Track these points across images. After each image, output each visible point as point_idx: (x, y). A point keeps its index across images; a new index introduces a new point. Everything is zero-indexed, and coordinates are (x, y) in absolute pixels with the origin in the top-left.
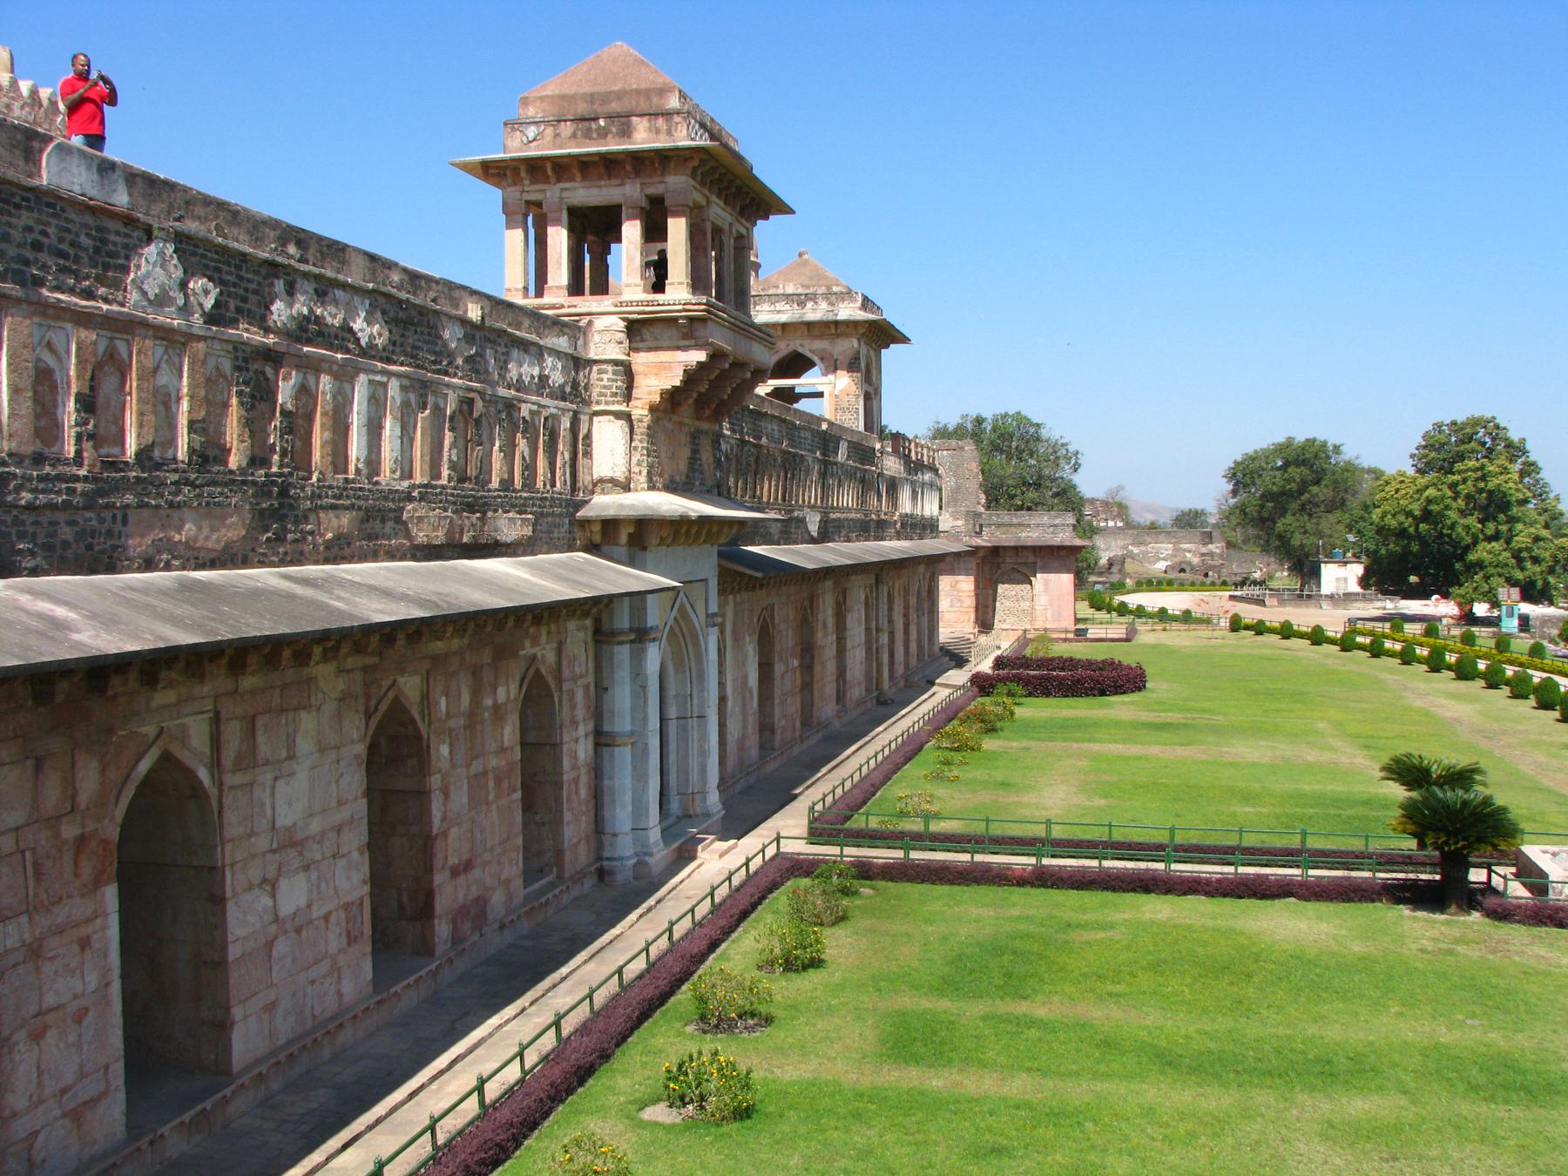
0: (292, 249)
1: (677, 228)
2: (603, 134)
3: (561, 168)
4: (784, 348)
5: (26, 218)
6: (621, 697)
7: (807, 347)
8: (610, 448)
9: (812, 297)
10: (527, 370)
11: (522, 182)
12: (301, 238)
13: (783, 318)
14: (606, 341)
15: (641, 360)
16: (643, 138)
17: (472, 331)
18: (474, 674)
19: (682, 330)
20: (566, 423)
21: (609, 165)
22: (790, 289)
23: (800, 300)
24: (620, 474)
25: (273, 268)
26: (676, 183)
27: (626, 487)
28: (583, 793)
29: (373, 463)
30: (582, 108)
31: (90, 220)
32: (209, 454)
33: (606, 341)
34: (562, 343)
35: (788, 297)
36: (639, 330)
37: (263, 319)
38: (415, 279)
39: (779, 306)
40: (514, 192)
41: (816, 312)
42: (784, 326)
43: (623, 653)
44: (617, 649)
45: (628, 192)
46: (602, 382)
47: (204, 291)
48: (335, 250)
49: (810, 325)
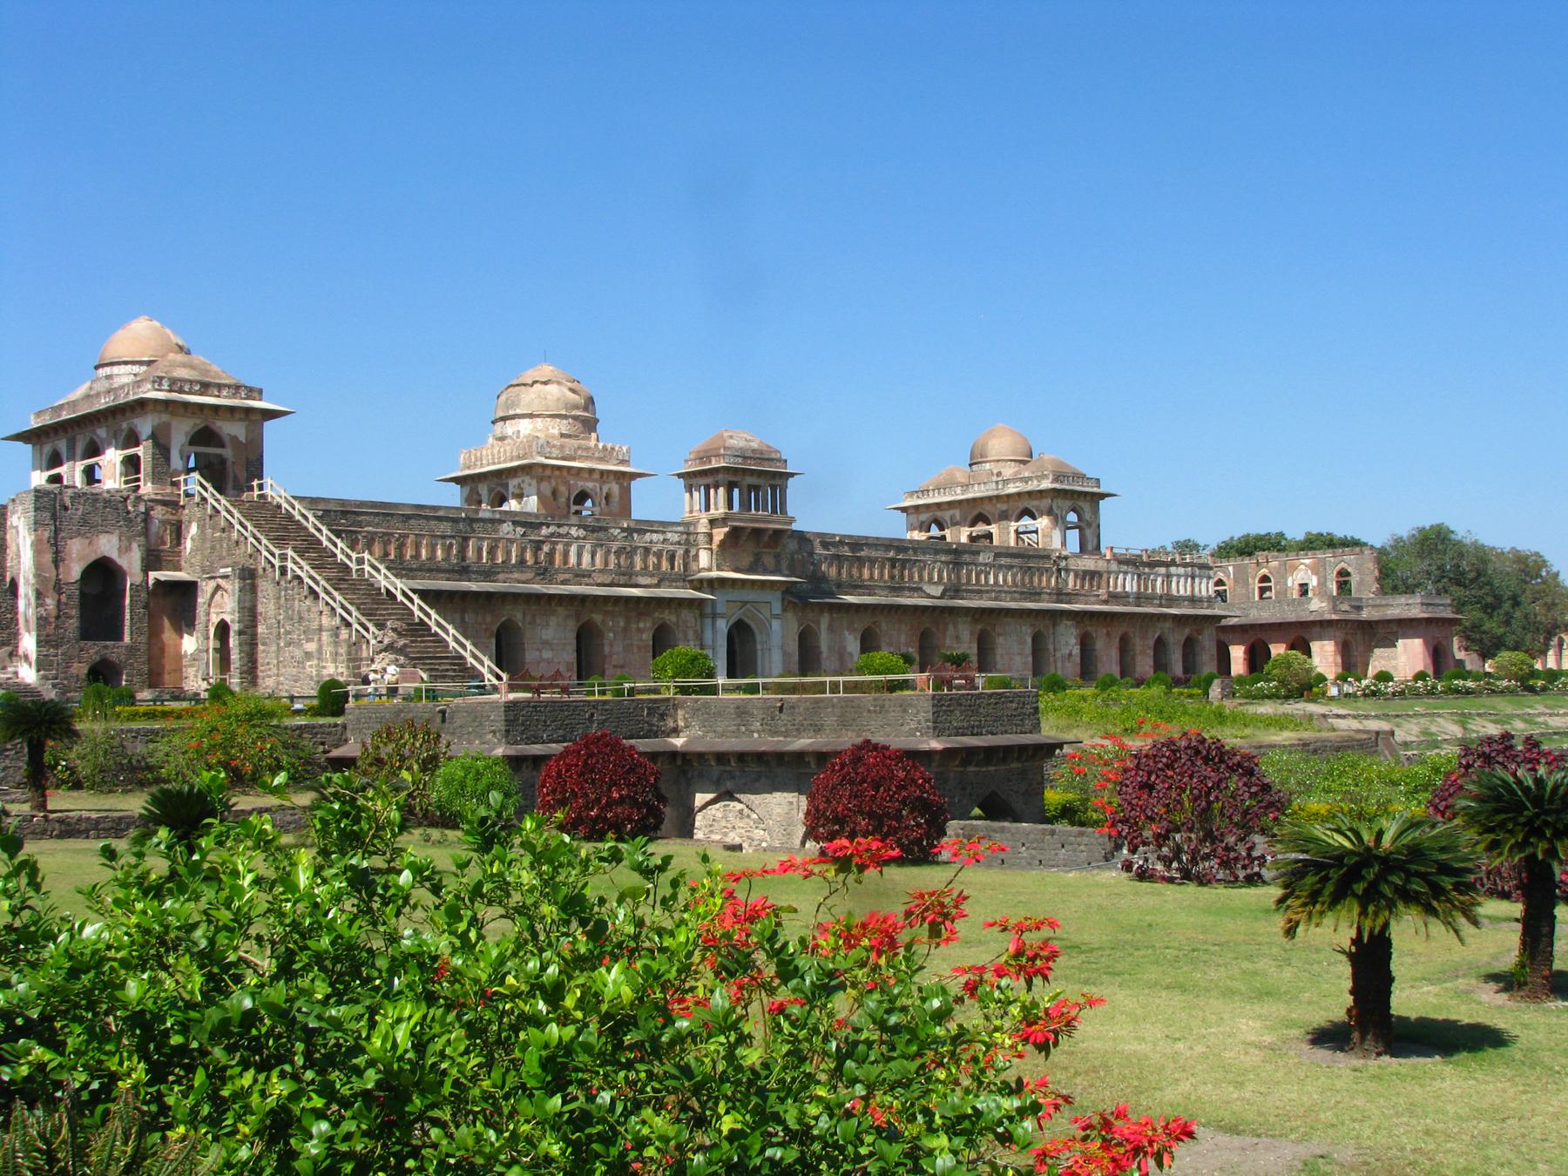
1: (736, 491)
4: (1022, 505)
6: (708, 635)
7: (1031, 504)
8: (704, 559)
9: (1030, 478)
11: (690, 479)
14: (703, 528)
15: (715, 531)
16: (715, 464)
19: (723, 521)
20: (680, 552)
26: (720, 477)
27: (710, 570)
29: (579, 563)
32: (522, 562)
34: (681, 529)
36: (713, 522)
42: (1019, 494)
43: (708, 621)
45: (710, 480)
46: (701, 538)
49: (1030, 493)
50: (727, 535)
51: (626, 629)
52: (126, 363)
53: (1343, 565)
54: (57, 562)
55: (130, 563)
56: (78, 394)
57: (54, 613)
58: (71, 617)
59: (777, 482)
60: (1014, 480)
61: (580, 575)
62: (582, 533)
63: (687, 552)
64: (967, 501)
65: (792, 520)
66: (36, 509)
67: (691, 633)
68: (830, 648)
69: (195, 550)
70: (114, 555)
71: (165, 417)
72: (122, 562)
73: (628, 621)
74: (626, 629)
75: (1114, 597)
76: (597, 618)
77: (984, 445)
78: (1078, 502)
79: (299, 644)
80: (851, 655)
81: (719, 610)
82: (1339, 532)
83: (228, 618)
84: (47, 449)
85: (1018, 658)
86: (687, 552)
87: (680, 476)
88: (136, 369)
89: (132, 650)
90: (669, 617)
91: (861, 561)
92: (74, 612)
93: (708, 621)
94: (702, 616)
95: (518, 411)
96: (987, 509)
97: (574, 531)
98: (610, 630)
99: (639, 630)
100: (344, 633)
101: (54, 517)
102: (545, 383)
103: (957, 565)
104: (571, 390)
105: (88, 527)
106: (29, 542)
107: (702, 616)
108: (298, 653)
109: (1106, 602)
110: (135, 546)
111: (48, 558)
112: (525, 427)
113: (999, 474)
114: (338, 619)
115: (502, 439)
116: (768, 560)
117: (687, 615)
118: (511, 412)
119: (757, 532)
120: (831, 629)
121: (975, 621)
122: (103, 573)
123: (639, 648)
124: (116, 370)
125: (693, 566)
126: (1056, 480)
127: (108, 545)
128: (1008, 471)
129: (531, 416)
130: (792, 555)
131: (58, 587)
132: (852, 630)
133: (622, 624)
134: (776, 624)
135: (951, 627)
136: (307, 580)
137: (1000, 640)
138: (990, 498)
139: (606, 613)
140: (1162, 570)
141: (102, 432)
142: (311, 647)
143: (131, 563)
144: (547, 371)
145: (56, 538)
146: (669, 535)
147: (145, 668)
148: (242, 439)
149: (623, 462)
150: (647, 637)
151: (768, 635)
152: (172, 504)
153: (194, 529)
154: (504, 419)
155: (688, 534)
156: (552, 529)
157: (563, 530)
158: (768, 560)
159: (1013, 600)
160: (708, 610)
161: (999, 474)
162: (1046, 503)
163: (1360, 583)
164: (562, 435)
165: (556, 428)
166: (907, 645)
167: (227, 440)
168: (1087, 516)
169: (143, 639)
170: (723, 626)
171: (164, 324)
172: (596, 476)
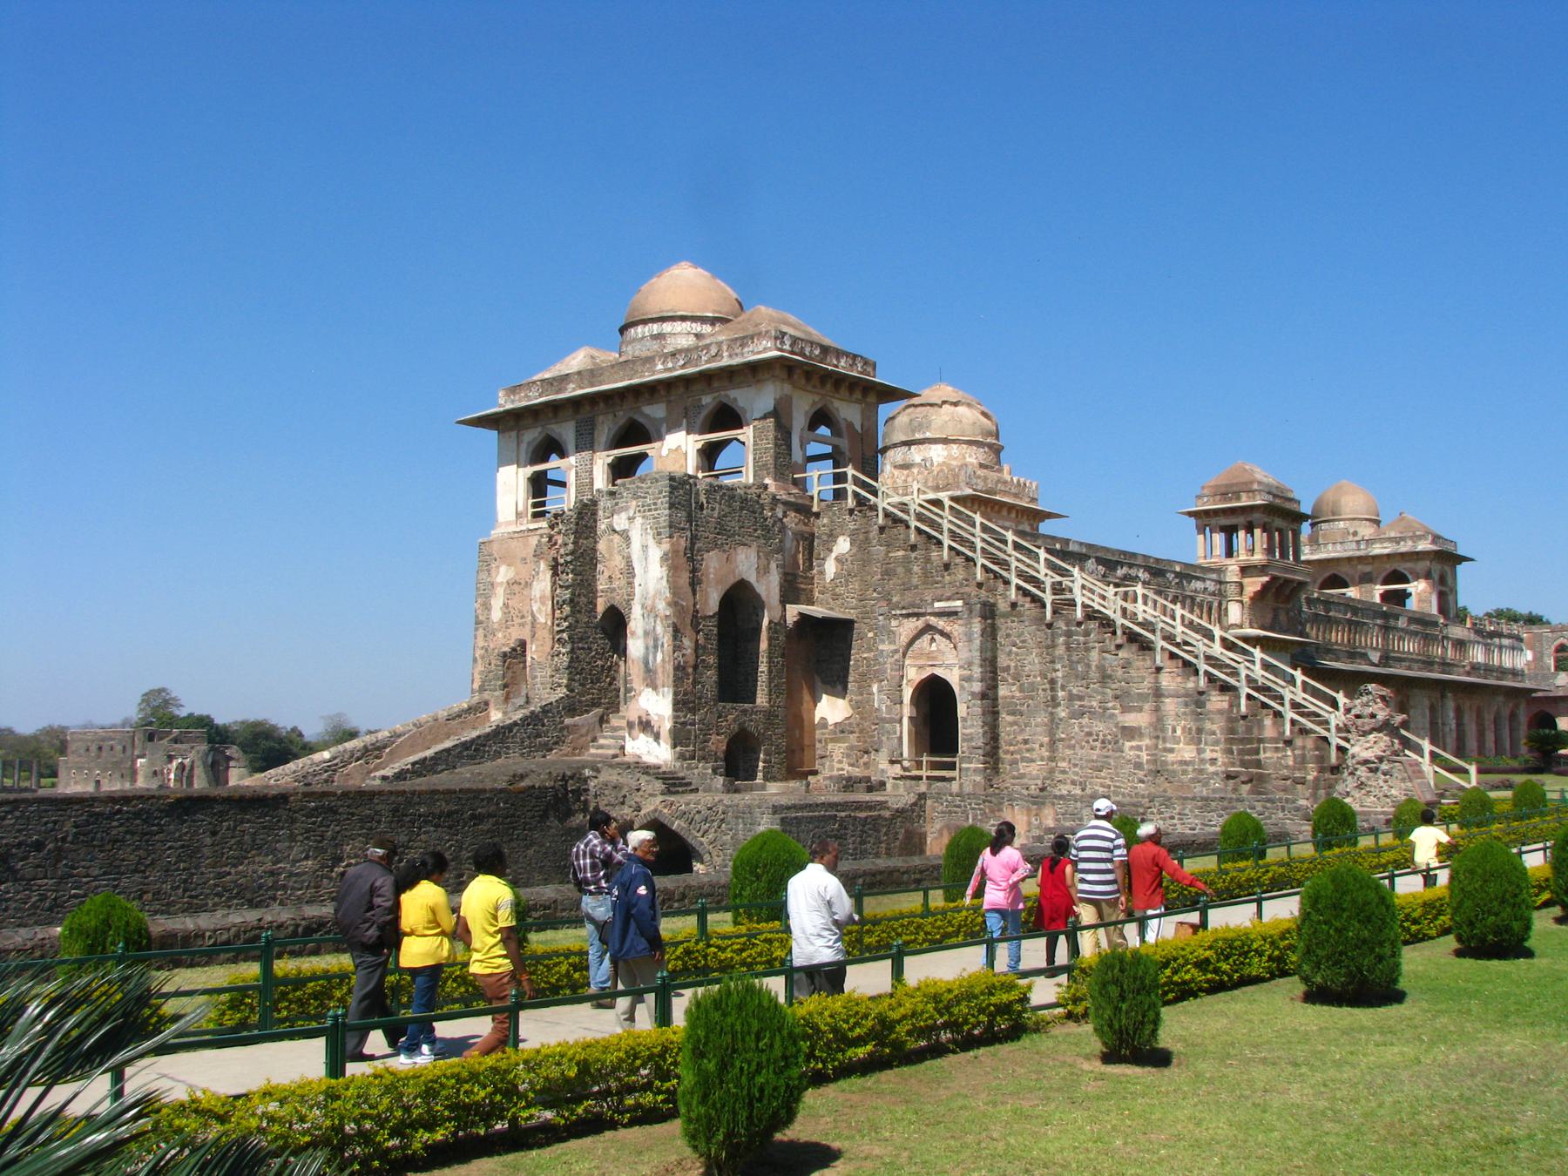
2: (1230, 500)
3: (1216, 512)
4: (1389, 567)
7: (1403, 567)
8: (1235, 613)
9: (1403, 539)
10: (1198, 585)
11: (1204, 519)
12: (1125, 553)
13: (1386, 551)
14: (1232, 574)
15: (1246, 581)
16: (1245, 502)
17: (1178, 575)
20: (1216, 604)
21: (1233, 511)
22: (1393, 535)
23: (1397, 540)
24: (1238, 622)
25: (1118, 563)
26: (1256, 516)
27: (1241, 627)
30: (1223, 490)
33: (1232, 574)
34: (1214, 576)
35: (1390, 539)
36: (1245, 570)
38: (1158, 561)
41: (1404, 547)
42: (1388, 556)
45: (1240, 520)
48: (1134, 555)
49: (1402, 555)
50: (1265, 587)
52: (683, 318)
53: (1561, 640)
54: (694, 583)
55: (768, 589)
56: (578, 364)
57: (692, 662)
58: (708, 667)
63: (1220, 604)
64: (1320, 561)
66: (672, 506)
69: (844, 576)
70: (752, 578)
71: (787, 388)
72: (761, 589)
75: (1475, 668)
77: (1336, 503)
78: (1443, 563)
79: (1104, 714)
82: (1523, 610)
83: (953, 677)
84: (532, 435)
86: (1220, 604)
87: (1190, 514)
88: (697, 327)
89: (770, 715)
91: (1330, 622)
92: (712, 660)
95: (928, 435)
96: (1343, 572)
100: (1217, 702)
101: (690, 520)
102: (955, 404)
104: (984, 414)
105: (725, 536)
106: (656, 553)
108: (1099, 727)
109: (1468, 674)
110: (773, 565)
111: (685, 578)
112: (937, 453)
113: (1355, 534)
114: (1202, 682)
115: (906, 466)
116: (1282, 617)
118: (918, 436)
122: (739, 604)
124: (667, 327)
126: (1433, 542)
127: (746, 563)
128: (1367, 531)
129: (945, 441)
131: (696, 620)
136: (1120, 621)
138: (1349, 559)
141: (655, 411)
142: (1139, 719)
143: (769, 587)
144: (946, 391)
145: (692, 549)
147: (783, 743)
148: (858, 428)
149: (1033, 500)
152: (804, 510)
153: (843, 545)
154: (908, 444)
155: (1221, 583)
157: (1133, 572)
158: (1282, 617)
159: (1420, 669)
161: (1355, 534)
162: (1423, 565)
164: (982, 466)
165: (973, 457)
167: (843, 425)
168: (1450, 581)
169: (781, 701)
171: (716, 272)
172: (1013, 515)
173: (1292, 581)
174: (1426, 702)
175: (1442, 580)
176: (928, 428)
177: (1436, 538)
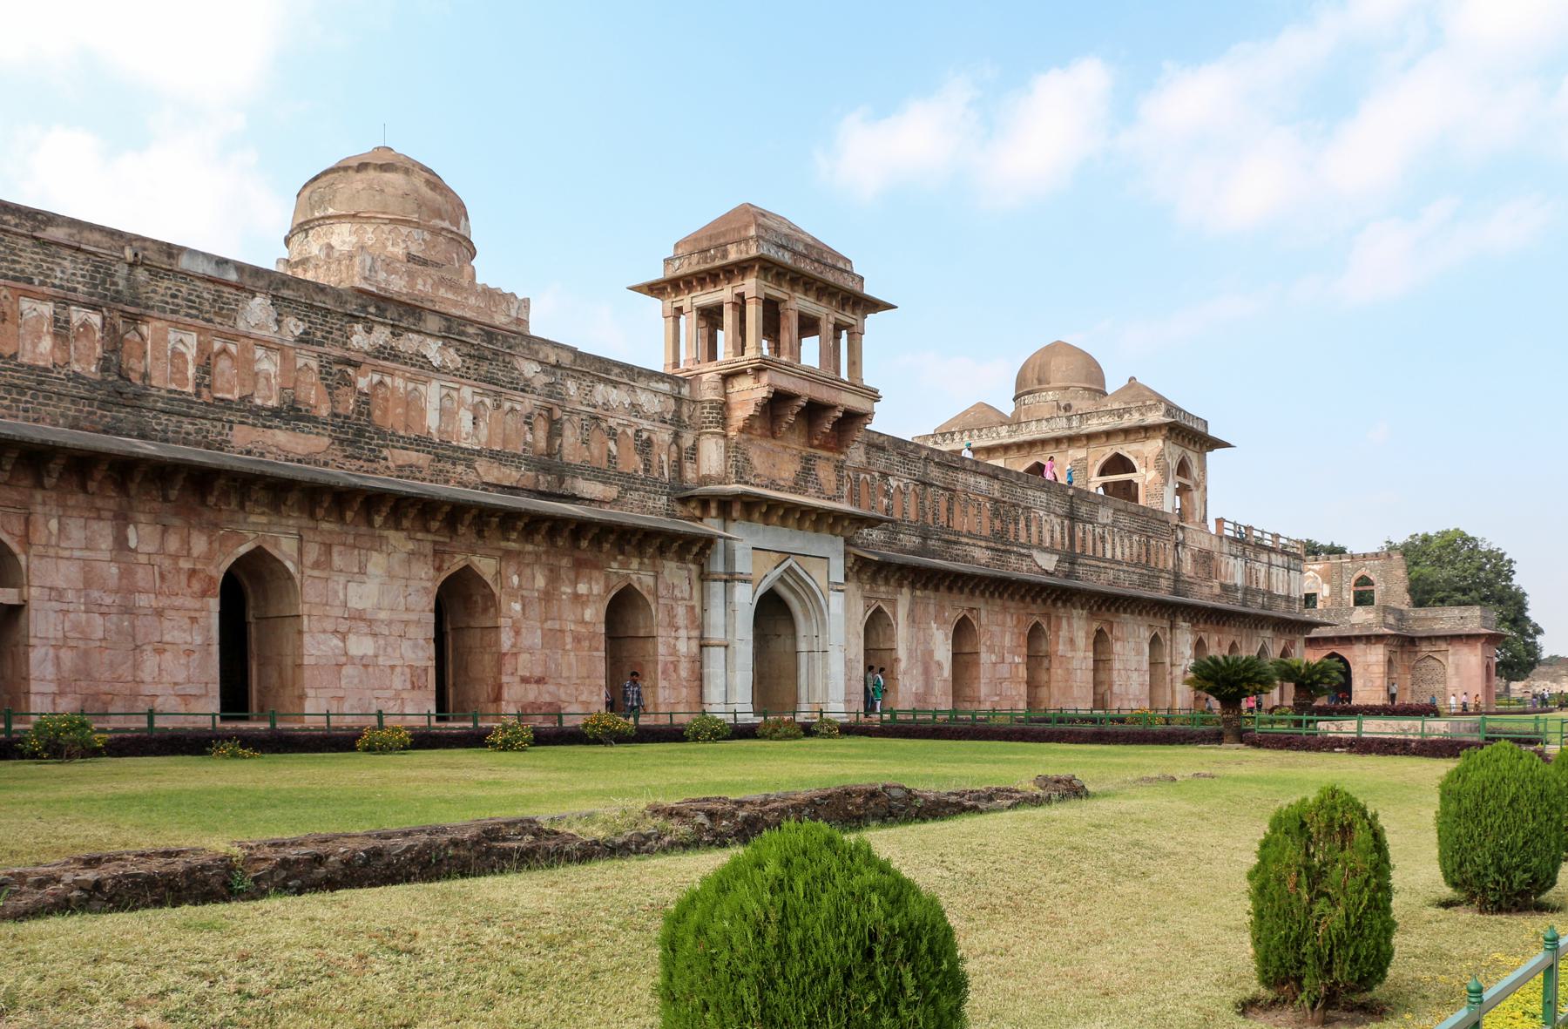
0: (372, 310)
5: (166, 283)
6: (716, 615)
18: (551, 571)
26: (750, 285)
28: (684, 673)
31: (211, 286)
34: (665, 387)
37: (345, 343)
39: (1104, 420)
40: (668, 303)
43: (717, 588)
44: (712, 584)
45: (724, 294)
47: (294, 326)
51: (548, 596)
59: (847, 317)
60: (1099, 414)
61: (444, 452)
62: (452, 358)
65: (874, 396)
67: (681, 611)
68: (910, 656)
73: (554, 577)
74: (548, 596)
76: (486, 566)
80: (939, 664)
81: (742, 565)
85: (1135, 675)
90: (639, 574)
93: (717, 588)
94: (704, 577)
97: (433, 350)
98: (514, 594)
99: (576, 597)
103: (1072, 517)
107: (704, 577)
117: (676, 576)
119: (815, 410)
120: (912, 618)
121: (1092, 615)
123: (577, 639)
125: (690, 474)
126: (1168, 412)
130: (857, 470)
132: (941, 621)
133: (540, 582)
134: (836, 602)
135: (1064, 623)
137: (1117, 647)
139: (507, 554)
140: (1264, 557)
146: (643, 398)
150: (594, 614)
151: (823, 624)
155: (679, 400)
156: (381, 335)
158: (825, 473)
160: (718, 566)
163: (1387, 592)
166: (1014, 654)
168: (1195, 472)
170: (745, 598)
173: (833, 407)
174: (1145, 634)
175: (1183, 469)
176: (331, 202)
177: (1171, 409)
